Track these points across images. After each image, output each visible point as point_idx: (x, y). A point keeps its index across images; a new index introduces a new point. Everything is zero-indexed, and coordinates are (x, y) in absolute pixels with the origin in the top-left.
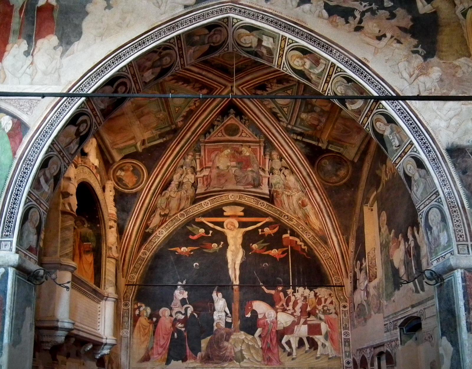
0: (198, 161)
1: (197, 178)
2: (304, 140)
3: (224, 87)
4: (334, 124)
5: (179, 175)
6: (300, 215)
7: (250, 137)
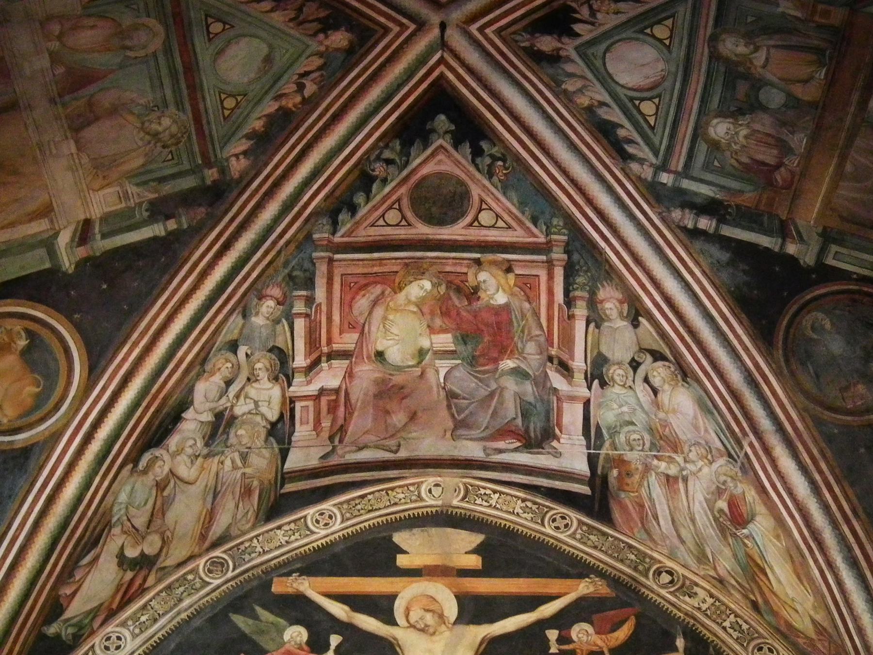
0: (300, 325)
1: (292, 401)
2: (728, 231)
3: (413, 27)
4: (843, 158)
5: (217, 380)
6: (726, 564)
7: (509, 227)
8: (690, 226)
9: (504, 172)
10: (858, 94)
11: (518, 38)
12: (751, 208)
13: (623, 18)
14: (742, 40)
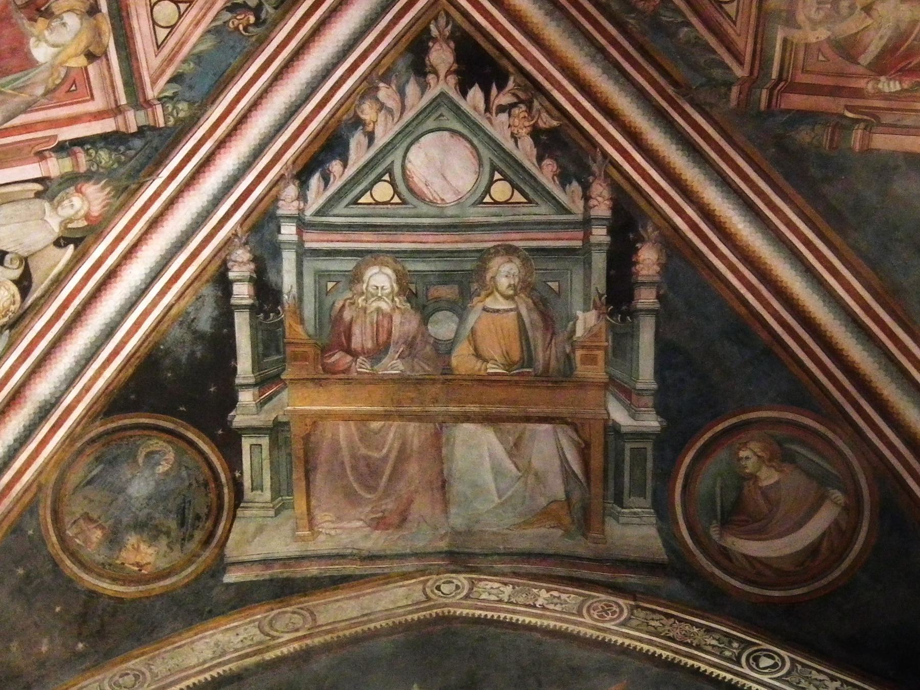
4: (386, 416)
8: (232, 275)
9: (241, 27)
10: (477, 409)
11: (442, 21)
12: (284, 337)
13: (509, 145)
14: (517, 280)
